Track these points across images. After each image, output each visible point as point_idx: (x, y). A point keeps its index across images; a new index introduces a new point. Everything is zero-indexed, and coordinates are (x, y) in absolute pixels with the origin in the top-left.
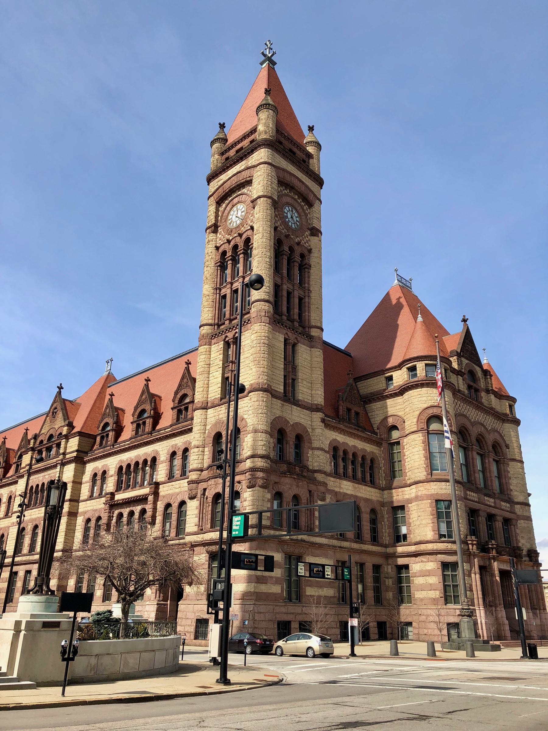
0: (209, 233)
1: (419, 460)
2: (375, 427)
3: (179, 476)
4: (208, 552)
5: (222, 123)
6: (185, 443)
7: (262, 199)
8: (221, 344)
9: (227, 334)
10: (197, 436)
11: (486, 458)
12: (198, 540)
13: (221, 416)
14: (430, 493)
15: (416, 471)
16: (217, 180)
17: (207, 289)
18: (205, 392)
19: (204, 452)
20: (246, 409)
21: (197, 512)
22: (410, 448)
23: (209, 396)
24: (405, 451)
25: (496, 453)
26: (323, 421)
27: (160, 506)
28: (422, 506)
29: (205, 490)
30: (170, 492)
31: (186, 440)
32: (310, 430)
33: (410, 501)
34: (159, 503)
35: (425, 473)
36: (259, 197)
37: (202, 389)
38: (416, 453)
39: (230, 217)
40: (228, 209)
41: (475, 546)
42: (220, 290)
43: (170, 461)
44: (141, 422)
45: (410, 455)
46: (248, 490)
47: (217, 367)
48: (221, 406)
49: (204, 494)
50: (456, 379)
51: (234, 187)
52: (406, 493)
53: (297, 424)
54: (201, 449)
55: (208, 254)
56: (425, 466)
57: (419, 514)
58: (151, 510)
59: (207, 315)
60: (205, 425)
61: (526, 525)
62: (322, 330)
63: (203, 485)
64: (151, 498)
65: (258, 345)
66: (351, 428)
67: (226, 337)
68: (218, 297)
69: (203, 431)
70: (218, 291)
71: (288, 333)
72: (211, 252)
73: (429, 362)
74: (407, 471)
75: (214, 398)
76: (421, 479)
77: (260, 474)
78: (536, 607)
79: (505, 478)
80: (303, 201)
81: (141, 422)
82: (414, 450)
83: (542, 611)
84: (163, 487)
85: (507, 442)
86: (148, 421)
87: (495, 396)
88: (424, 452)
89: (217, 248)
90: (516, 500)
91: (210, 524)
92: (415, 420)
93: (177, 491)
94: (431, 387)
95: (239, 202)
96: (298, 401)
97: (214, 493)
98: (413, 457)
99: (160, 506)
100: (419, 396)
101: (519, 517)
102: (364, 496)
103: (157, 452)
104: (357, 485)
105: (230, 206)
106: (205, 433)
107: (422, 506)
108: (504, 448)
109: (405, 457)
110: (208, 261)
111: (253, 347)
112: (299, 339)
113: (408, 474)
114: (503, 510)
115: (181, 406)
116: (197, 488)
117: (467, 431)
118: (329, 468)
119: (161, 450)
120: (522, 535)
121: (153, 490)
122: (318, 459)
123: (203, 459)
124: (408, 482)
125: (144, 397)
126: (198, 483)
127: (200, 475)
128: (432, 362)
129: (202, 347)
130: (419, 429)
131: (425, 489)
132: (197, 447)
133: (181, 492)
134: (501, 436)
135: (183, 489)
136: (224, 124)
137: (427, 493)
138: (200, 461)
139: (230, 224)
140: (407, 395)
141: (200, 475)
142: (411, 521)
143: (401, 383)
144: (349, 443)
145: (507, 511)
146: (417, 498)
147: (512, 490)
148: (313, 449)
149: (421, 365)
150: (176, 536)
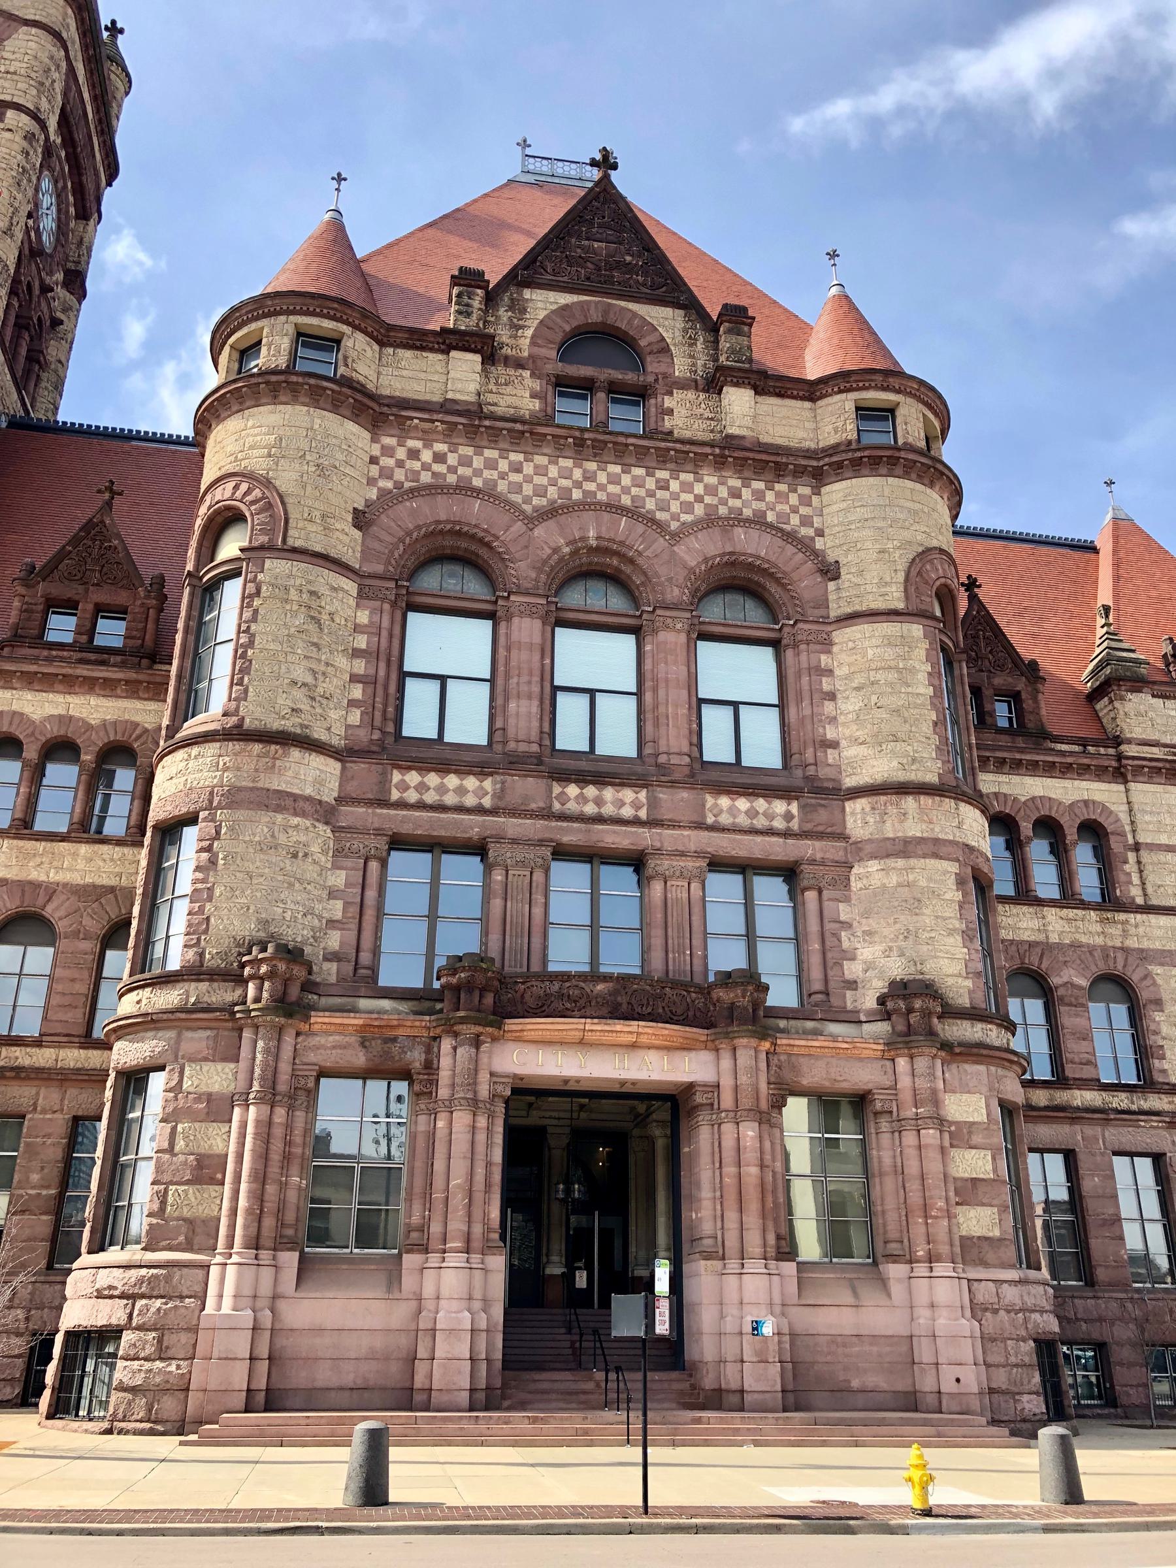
11: (648, 639)
25: (771, 609)
41: (267, 984)
50: (439, 367)
61: (894, 879)
66: (35, 660)
78: (893, 1247)
79: (799, 700)
83: (921, 1269)
87: (759, 391)
90: (849, 782)
101: (859, 851)
102: (75, 878)
108: (806, 582)
114: (713, 828)
117: (488, 545)
120: (872, 924)
134: (790, 537)
144: (28, 710)
145: (770, 832)
147: (835, 745)
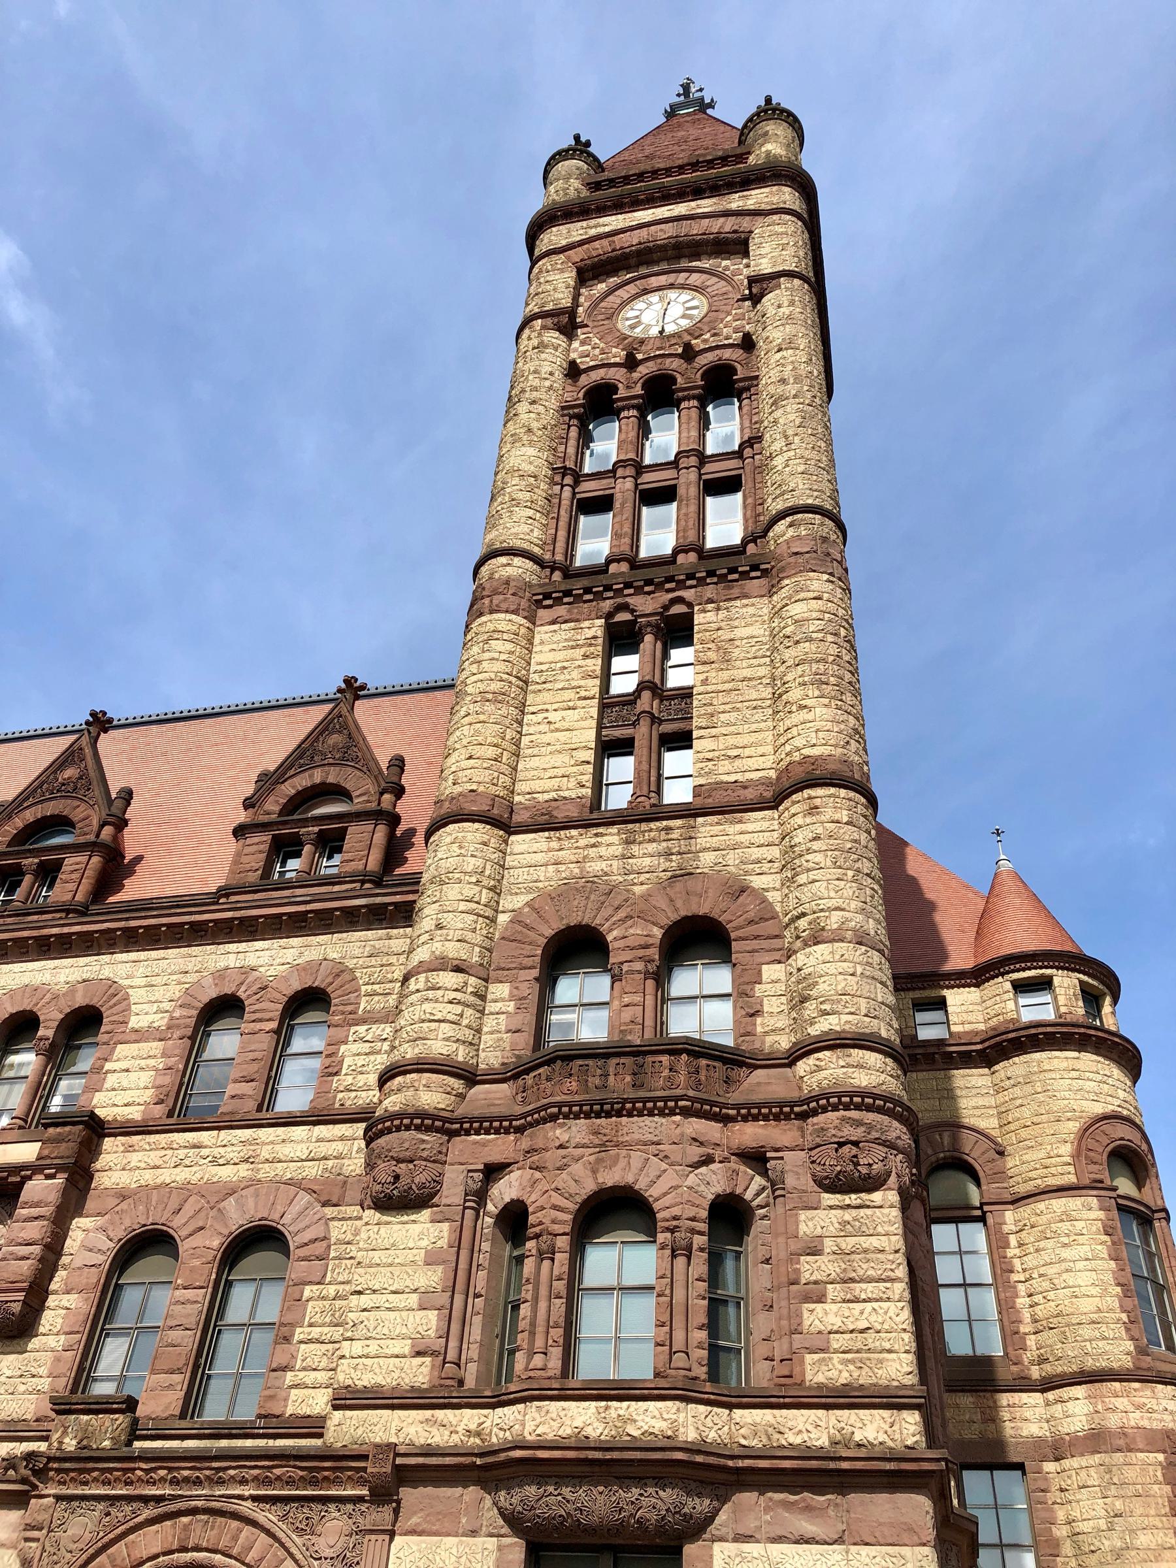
0: (544, 327)
1: (1094, 1291)
3: (251, 1105)
4: (513, 1521)
5: (583, 139)
7: (797, 282)
8: (595, 628)
9: (628, 599)
10: (458, 923)
12: (438, 1438)
13: (596, 867)
14: (1156, 1425)
15: (1087, 1332)
16: (584, 224)
17: (529, 457)
18: (504, 768)
19: (483, 998)
20: (756, 853)
21: (433, 1277)
22: (1049, 1244)
23: (520, 787)
24: (1010, 1253)
27: (89, 1240)
28: (1130, 1474)
29: (493, 1172)
30: (181, 1175)
31: (313, 954)
33: (1058, 1449)
34: (78, 1222)
35: (1130, 1346)
36: (790, 274)
37: (491, 752)
38: (1080, 1265)
40: (623, 293)
42: (577, 482)
43: (192, 1038)
44: (30, 862)
45: (1051, 1271)
46: (829, 1199)
47: (569, 694)
48: (601, 830)
49: (481, 1196)
51: (662, 248)
52: (1028, 1414)
54: (472, 980)
55: (535, 372)
56: (1124, 1317)
57: (1119, 1504)
58: (36, 1250)
59: (526, 528)
60: (496, 890)
63: (484, 1144)
64: (42, 1191)
65: (830, 638)
67: (625, 607)
69: (489, 912)
70: (568, 480)
72: (551, 374)
73: (1090, 981)
74: (1023, 1329)
75: (553, 795)
76: (1115, 1365)
81: (30, 862)
82: (1066, 1253)
84: (130, 1149)
86: (72, 862)
88: (1113, 1264)
89: (573, 371)
91: (556, 1353)
92: (1066, 1149)
93: (226, 1173)
94: (1106, 1057)
95: (672, 286)
97: (589, 1187)
98: (1070, 1279)
99: (89, 1240)
100: (1074, 1074)
103: (113, 990)
105: (632, 289)
106: (493, 920)
107: (1130, 1474)
109: (1014, 1277)
110: (535, 389)
111: (811, 640)
113: (1031, 1341)
115: (305, 822)
116: (439, 1160)
119: (143, 982)
121: (66, 1150)
123: (479, 1031)
124: (1035, 1373)
125: (70, 773)
126: (452, 1134)
127: (461, 1096)
128: (1095, 983)
129: (502, 616)
130: (1087, 1182)
131: (1139, 1407)
132: (458, 969)
133: (253, 1183)
135: (267, 1172)
137: (1145, 1423)
138: (468, 1034)
139: (632, 327)
140: (1016, 1066)
141: (461, 1096)
143: (982, 1027)
146: (1097, 1440)
149: (1067, 982)
150: (183, 1416)
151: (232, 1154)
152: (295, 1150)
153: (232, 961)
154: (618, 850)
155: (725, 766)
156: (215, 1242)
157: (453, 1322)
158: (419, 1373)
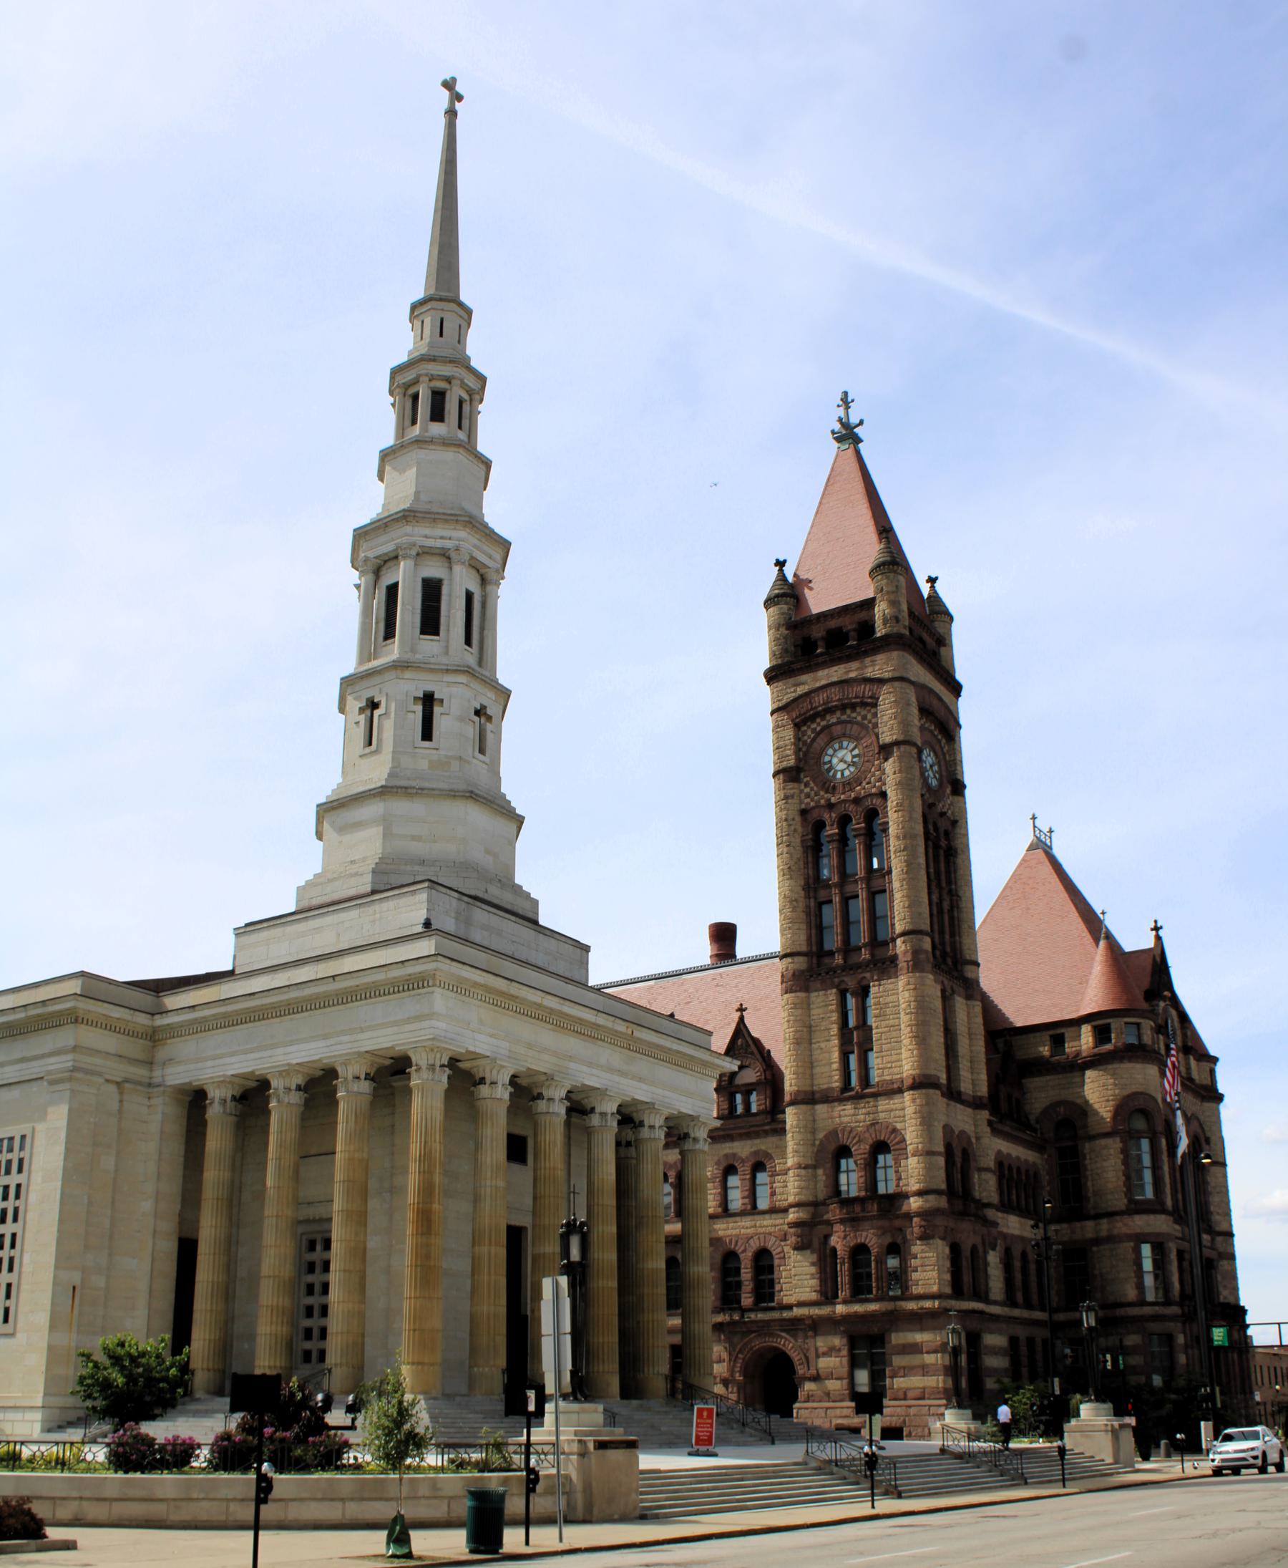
2: (1032, 1118)
6: (756, 1153)
8: (832, 995)
13: (845, 1119)
26: (990, 1123)
30: (734, 1232)
32: (973, 1140)
36: (897, 743)
39: (827, 759)
53: (962, 1132)
62: (978, 965)
68: (812, 904)
71: (946, 982)
74: (1090, 1194)
77: (940, 1221)
80: (940, 732)
85: (1208, 1134)
89: (804, 813)
90: (1217, 1229)
95: (844, 735)
96: (959, 1093)
104: (1023, 1220)
112: (955, 987)
118: (995, 1199)
122: (986, 1187)
124: (1092, 1212)
135: (760, 1230)
136: (785, 561)
142: (1097, 1272)
148: (980, 1170)
151: (748, 1224)
152: (767, 1222)
153: (727, 1151)
154: (852, 1112)
155: (886, 1072)
156: (750, 1254)
157: (823, 1281)
158: (814, 1296)
